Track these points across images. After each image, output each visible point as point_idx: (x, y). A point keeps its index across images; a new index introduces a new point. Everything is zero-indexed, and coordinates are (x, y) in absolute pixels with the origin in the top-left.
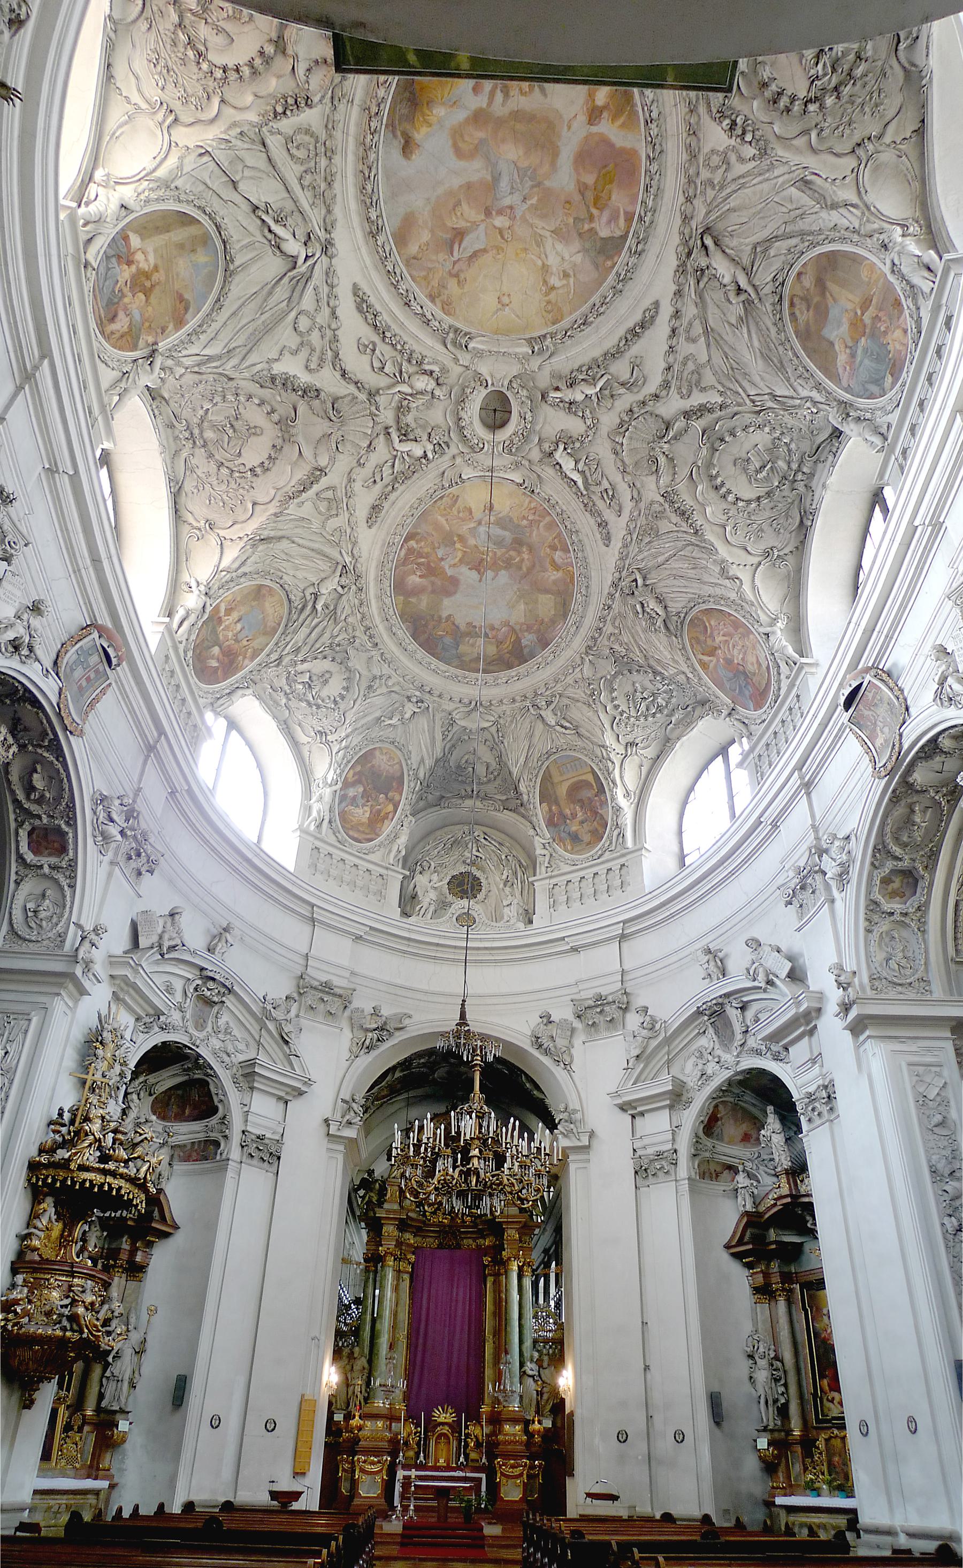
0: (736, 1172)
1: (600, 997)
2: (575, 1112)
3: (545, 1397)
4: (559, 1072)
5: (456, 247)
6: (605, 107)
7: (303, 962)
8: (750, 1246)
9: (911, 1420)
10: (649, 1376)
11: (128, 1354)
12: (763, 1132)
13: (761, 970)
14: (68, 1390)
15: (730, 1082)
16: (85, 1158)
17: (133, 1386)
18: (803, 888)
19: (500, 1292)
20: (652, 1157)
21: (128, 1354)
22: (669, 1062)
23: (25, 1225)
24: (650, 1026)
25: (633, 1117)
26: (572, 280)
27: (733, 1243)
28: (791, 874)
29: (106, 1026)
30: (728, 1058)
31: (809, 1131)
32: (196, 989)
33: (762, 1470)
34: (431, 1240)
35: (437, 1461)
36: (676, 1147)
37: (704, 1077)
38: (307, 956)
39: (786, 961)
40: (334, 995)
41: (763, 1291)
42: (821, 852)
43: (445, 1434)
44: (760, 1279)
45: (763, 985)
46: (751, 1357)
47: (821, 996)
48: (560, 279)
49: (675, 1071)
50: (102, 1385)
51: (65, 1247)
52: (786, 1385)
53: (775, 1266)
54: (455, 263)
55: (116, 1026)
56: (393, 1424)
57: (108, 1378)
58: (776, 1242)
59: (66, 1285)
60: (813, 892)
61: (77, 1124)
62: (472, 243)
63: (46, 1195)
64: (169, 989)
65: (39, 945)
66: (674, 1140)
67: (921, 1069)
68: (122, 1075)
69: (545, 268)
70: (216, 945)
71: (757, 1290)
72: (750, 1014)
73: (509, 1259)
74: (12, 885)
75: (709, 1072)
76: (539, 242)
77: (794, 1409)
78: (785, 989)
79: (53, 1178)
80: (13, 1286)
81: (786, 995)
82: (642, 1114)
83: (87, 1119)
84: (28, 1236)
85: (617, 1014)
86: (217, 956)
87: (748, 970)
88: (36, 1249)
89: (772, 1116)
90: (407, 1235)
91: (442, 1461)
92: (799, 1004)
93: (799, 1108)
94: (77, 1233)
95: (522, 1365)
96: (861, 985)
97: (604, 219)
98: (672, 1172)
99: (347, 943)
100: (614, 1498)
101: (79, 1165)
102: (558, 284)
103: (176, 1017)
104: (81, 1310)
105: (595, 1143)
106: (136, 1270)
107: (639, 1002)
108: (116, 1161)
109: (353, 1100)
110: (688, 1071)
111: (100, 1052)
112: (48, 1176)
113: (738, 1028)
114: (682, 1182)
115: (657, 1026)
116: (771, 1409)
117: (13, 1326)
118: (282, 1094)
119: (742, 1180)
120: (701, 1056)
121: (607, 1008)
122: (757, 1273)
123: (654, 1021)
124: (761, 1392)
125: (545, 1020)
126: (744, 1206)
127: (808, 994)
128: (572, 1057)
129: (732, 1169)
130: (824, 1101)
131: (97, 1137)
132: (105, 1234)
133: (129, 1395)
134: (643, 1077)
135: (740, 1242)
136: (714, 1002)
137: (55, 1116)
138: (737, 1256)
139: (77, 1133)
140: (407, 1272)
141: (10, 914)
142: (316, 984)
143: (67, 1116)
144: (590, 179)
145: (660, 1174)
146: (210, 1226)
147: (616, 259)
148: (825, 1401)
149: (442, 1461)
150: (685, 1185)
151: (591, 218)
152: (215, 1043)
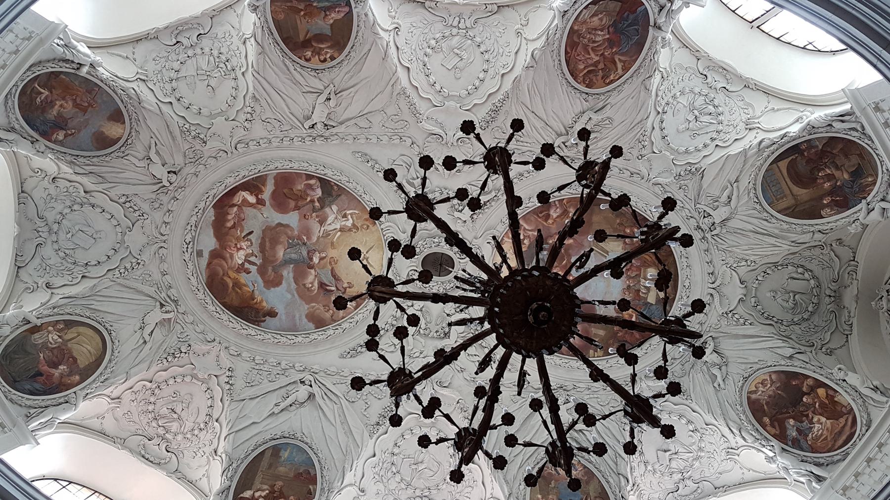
5: (328, 288)
6: (257, 196)
26: (348, 212)
48: (348, 220)
54: (338, 289)
62: (327, 279)
69: (341, 230)
76: (327, 234)
97: (312, 193)
102: (351, 221)
144: (292, 204)
147: (333, 184)
151: (312, 201)
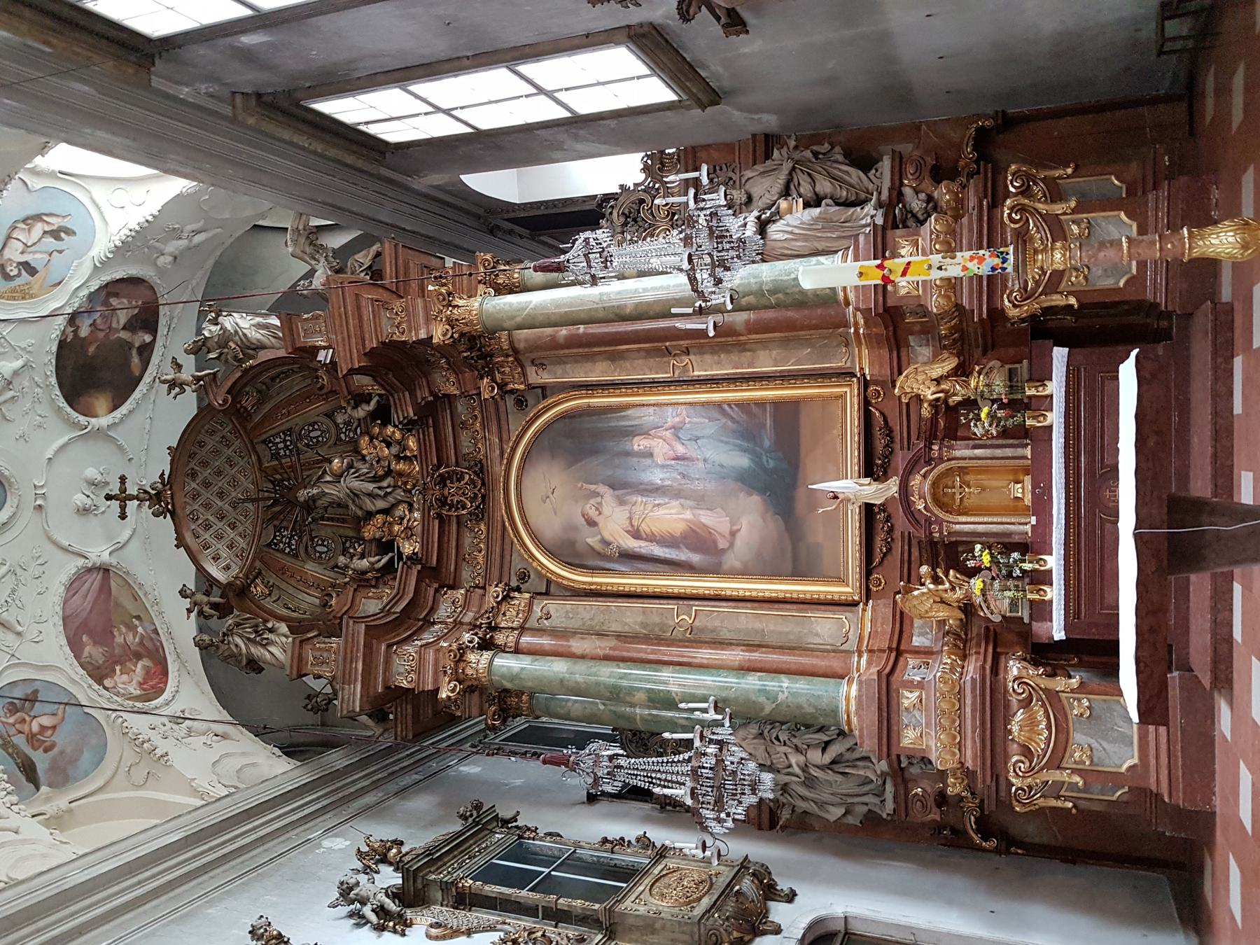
3: (824, 186)
19: (554, 345)
34: (468, 539)
35: (1016, 507)
43: (934, 485)
56: (917, 641)
73: (451, 322)
91: (1017, 490)
140: (530, 605)
149: (1017, 490)
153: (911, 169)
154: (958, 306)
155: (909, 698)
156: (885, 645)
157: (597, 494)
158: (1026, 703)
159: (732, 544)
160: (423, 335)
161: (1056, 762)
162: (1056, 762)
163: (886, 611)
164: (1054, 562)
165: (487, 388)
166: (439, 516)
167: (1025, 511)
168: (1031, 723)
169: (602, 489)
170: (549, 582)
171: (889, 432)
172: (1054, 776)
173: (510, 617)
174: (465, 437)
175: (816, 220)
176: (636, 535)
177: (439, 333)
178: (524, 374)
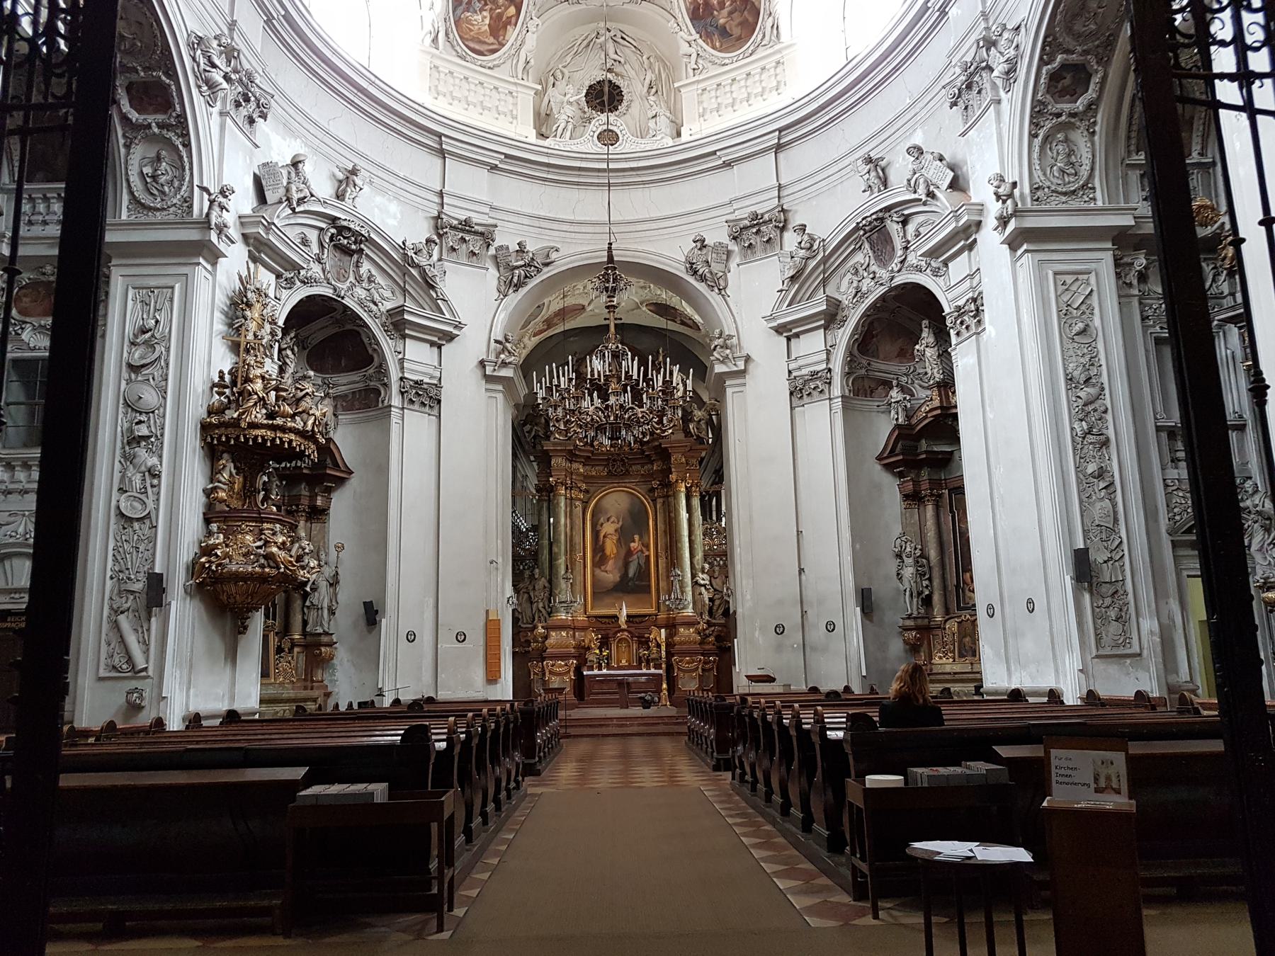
0: (891, 388)
1: (755, 216)
2: (730, 337)
3: (717, 602)
4: (713, 297)
7: (437, 200)
8: (901, 457)
9: (1030, 601)
10: (803, 577)
11: (323, 585)
12: (917, 347)
13: (921, 181)
14: (274, 619)
15: (883, 298)
16: (253, 416)
17: (332, 612)
18: (969, 87)
20: (806, 377)
21: (323, 585)
22: (825, 282)
23: (208, 482)
24: (808, 245)
25: (789, 339)
27: (885, 455)
28: (958, 71)
29: (248, 286)
30: (883, 274)
31: (957, 345)
32: (331, 239)
33: (906, 651)
34: (601, 468)
35: (619, 661)
36: (831, 366)
37: (859, 294)
38: (441, 194)
39: (948, 171)
40: (476, 233)
41: (913, 498)
42: (990, 44)
44: (910, 486)
45: (924, 198)
46: (899, 556)
47: (981, 208)
49: (831, 290)
50: (304, 613)
51: (250, 498)
52: (930, 579)
53: (925, 474)
55: (258, 286)
56: (577, 634)
57: (308, 607)
58: (926, 452)
59: (257, 531)
60: (979, 92)
61: (239, 386)
63: (223, 452)
64: (305, 242)
65: (165, 213)
66: (828, 360)
67: (1069, 279)
68: (273, 334)
70: (345, 191)
71: (906, 497)
72: (911, 228)
73: (677, 481)
74: (123, 150)
75: (864, 289)
77: (937, 598)
78: (945, 201)
79: (227, 436)
80: (210, 534)
81: (947, 208)
82: (797, 335)
83: (248, 380)
84: (214, 489)
85: (774, 234)
86: (348, 201)
87: (909, 181)
88: (222, 501)
89: (927, 330)
90: (575, 466)
91: (624, 661)
92: (957, 218)
93: (948, 322)
94: (259, 484)
95: (693, 576)
96: (1022, 195)
98: (826, 391)
99: (484, 173)
100: (772, 680)
101: (249, 423)
103: (316, 269)
104: (274, 549)
105: (751, 367)
106: (318, 514)
107: (796, 220)
108: (283, 417)
109: (507, 340)
110: (843, 288)
111: (248, 313)
112: (221, 436)
113: (898, 243)
114: (836, 401)
115: (815, 247)
116: (915, 600)
117: (216, 567)
118: (435, 339)
119: (895, 394)
120: (856, 273)
121: (763, 228)
122: (908, 481)
123: (812, 239)
124: (907, 586)
125: (699, 244)
126: (897, 419)
127: (968, 207)
128: (726, 281)
129: (888, 385)
130: (972, 314)
131: (261, 396)
132: (284, 483)
133: (330, 620)
134: (798, 298)
135: (892, 451)
136: (874, 217)
137: (217, 380)
138: (889, 467)
139: (240, 394)
141: (128, 181)
142: (455, 222)
143: (227, 378)
145: (815, 393)
146: (382, 469)
148: (967, 592)
149: (624, 661)
150: (838, 403)
152: (360, 292)
153: (720, 629)
154: (675, 645)
155: (564, 634)
156: (576, 625)
157: (619, 521)
158: (566, 665)
159: (603, 571)
160: (673, 470)
161: (551, 673)
162: (551, 673)
163: (586, 624)
164: (605, 671)
165: (655, 484)
166: (609, 459)
167: (618, 664)
168: (561, 666)
169: (621, 523)
170: (587, 502)
171: (640, 623)
172: (532, 673)
173: (574, 493)
174: (639, 466)
175: (704, 602)
176: (604, 537)
177: (673, 477)
178: (660, 497)
